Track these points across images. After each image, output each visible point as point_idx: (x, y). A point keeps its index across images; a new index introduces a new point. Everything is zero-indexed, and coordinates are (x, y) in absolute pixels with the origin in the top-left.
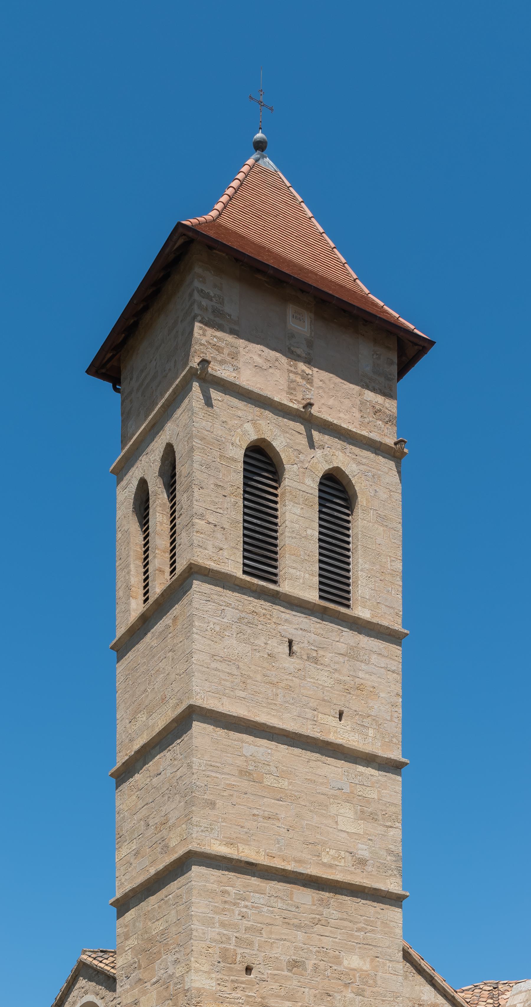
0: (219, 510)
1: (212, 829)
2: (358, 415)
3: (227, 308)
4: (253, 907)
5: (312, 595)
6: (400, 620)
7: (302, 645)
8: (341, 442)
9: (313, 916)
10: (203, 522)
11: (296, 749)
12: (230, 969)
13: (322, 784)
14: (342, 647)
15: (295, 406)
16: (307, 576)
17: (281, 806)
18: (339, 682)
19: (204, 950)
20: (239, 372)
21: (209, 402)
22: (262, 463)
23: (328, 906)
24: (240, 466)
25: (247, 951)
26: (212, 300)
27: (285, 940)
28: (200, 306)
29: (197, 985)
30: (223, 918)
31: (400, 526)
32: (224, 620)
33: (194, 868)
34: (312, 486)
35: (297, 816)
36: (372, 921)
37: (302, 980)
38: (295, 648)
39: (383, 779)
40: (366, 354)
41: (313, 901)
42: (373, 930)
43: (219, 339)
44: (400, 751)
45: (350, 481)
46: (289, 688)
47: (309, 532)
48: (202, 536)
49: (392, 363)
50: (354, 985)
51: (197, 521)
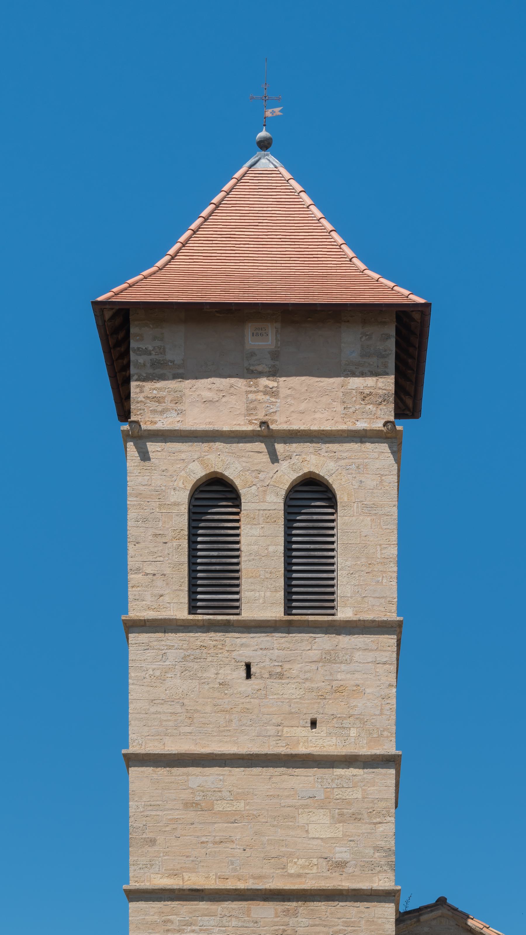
0: (158, 559)
1: (152, 865)
2: (340, 408)
4: (201, 930)
5: (276, 612)
6: (394, 608)
7: (262, 665)
8: (314, 445)
9: (277, 928)
10: (140, 575)
13: (288, 797)
14: (315, 654)
15: (250, 428)
16: (268, 594)
17: (236, 828)
18: (311, 690)
20: (185, 414)
21: (145, 456)
22: (214, 496)
23: (296, 915)
26: (150, 354)
31: (395, 509)
32: (167, 663)
34: (276, 502)
35: (256, 833)
36: (354, 922)
38: (253, 670)
40: (350, 341)
41: (276, 913)
43: (160, 389)
44: (393, 743)
45: (327, 481)
46: (246, 711)
48: (139, 589)
49: (388, 337)
51: (133, 576)
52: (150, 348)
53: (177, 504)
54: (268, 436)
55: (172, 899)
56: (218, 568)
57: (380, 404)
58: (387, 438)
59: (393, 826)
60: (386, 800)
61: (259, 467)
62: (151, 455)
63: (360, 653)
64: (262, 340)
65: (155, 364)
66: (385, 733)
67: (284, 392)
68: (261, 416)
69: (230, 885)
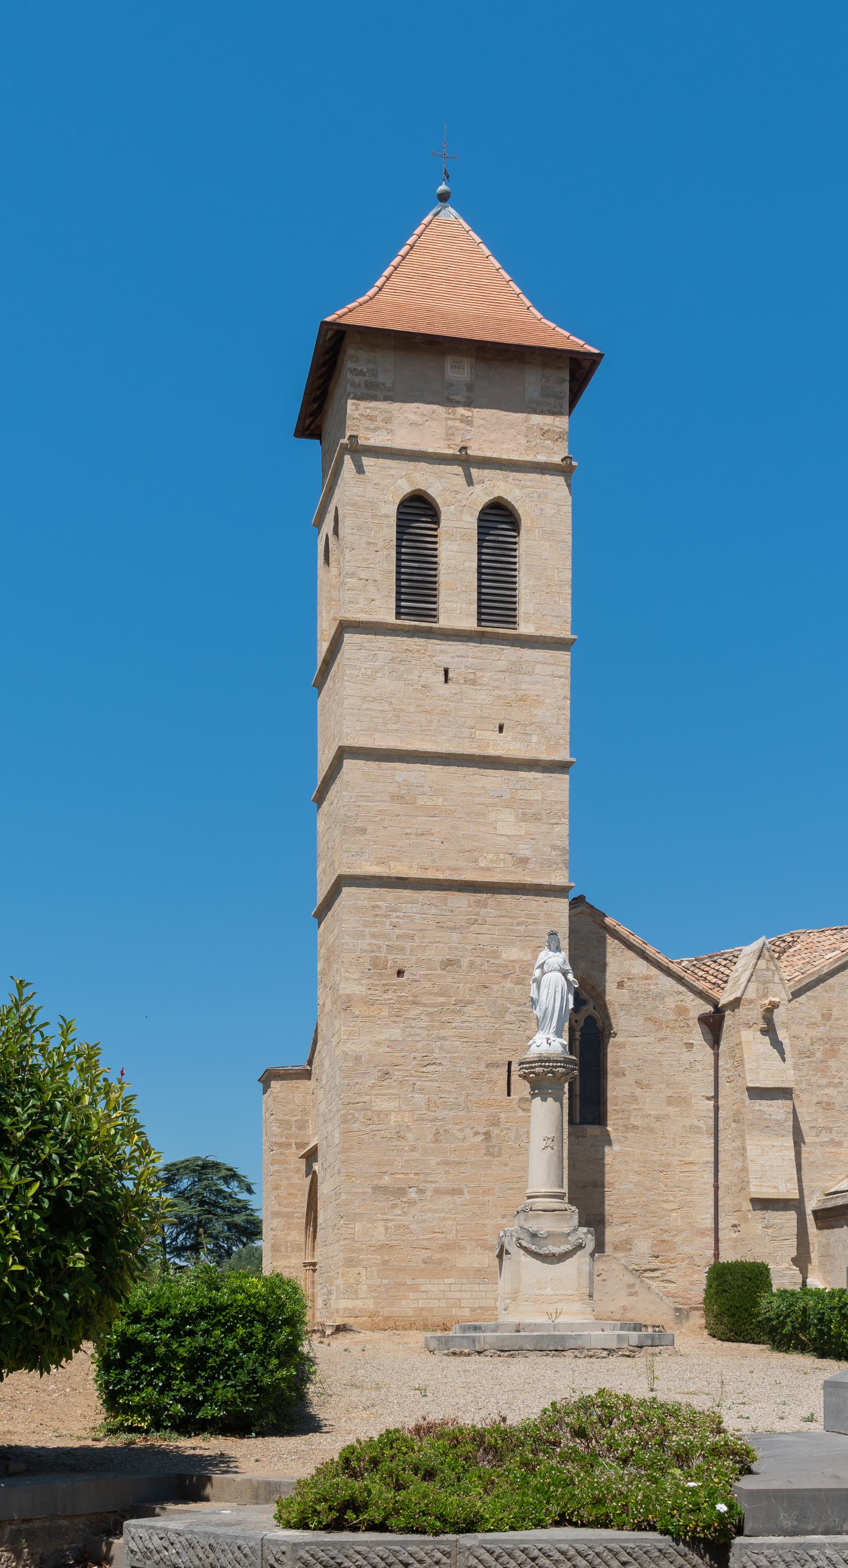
0: (371, 566)
2: (524, 441)
3: (381, 379)
4: (405, 916)
5: (470, 623)
6: (568, 627)
8: (503, 472)
10: (355, 580)
11: (451, 768)
12: (381, 974)
13: (480, 795)
14: (502, 664)
15: (451, 452)
16: (464, 606)
17: (436, 821)
18: (499, 697)
19: (354, 961)
21: (360, 470)
22: (418, 511)
23: (485, 906)
24: (393, 521)
25: (399, 956)
26: (365, 375)
27: (439, 942)
28: (353, 384)
29: (347, 991)
30: (373, 930)
32: (378, 663)
33: (344, 889)
34: (471, 522)
35: (452, 828)
36: (534, 915)
37: (456, 977)
38: (450, 675)
39: (548, 780)
40: (533, 381)
41: (469, 904)
42: (535, 923)
44: (568, 751)
45: (513, 506)
46: (445, 713)
47: (467, 564)
49: (563, 381)
50: (513, 975)
51: (348, 580)
52: (365, 370)
53: (386, 516)
54: (466, 461)
55: (380, 886)
56: (419, 578)
57: (557, 440)
58: (563, 472)
59: (567, 827)
60: (561, 802)
61: (457, 488)
62: (366, 469)
63: (540, 666)
64: (459, 372)
65: (370, 385)
66: (561, 741)
67: (477, 422)
68: (458, 441)
69: (430, 875)
